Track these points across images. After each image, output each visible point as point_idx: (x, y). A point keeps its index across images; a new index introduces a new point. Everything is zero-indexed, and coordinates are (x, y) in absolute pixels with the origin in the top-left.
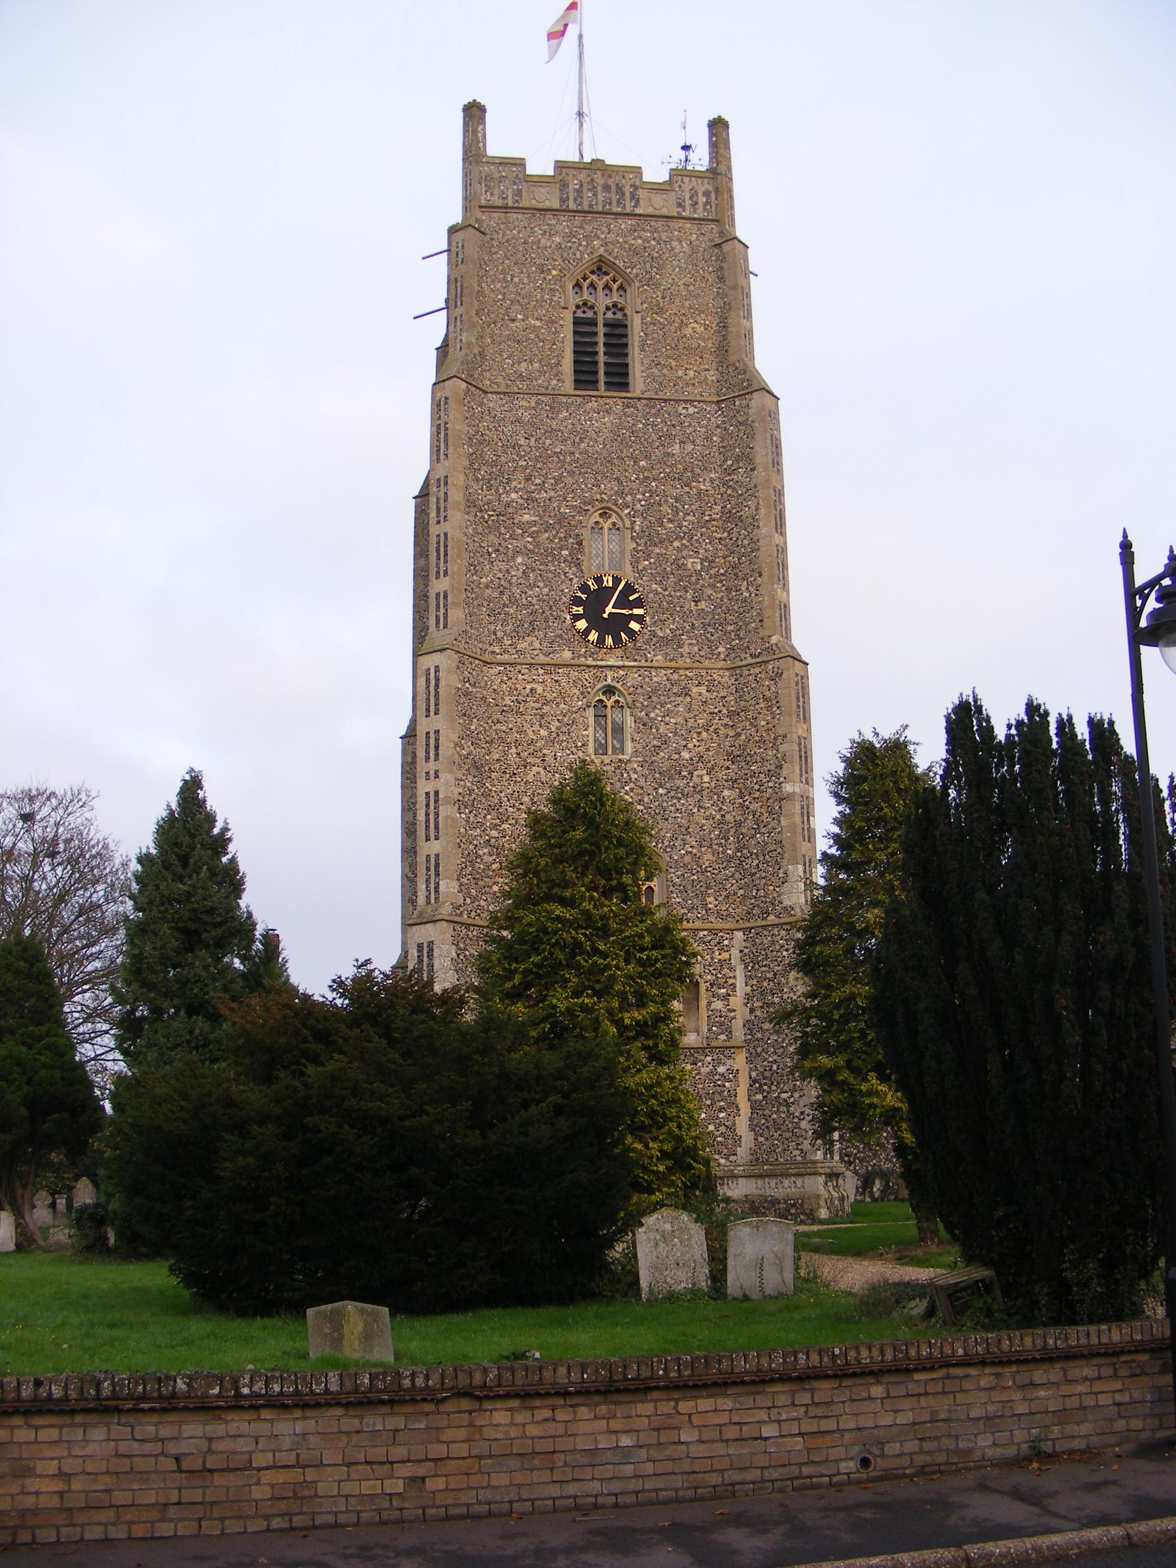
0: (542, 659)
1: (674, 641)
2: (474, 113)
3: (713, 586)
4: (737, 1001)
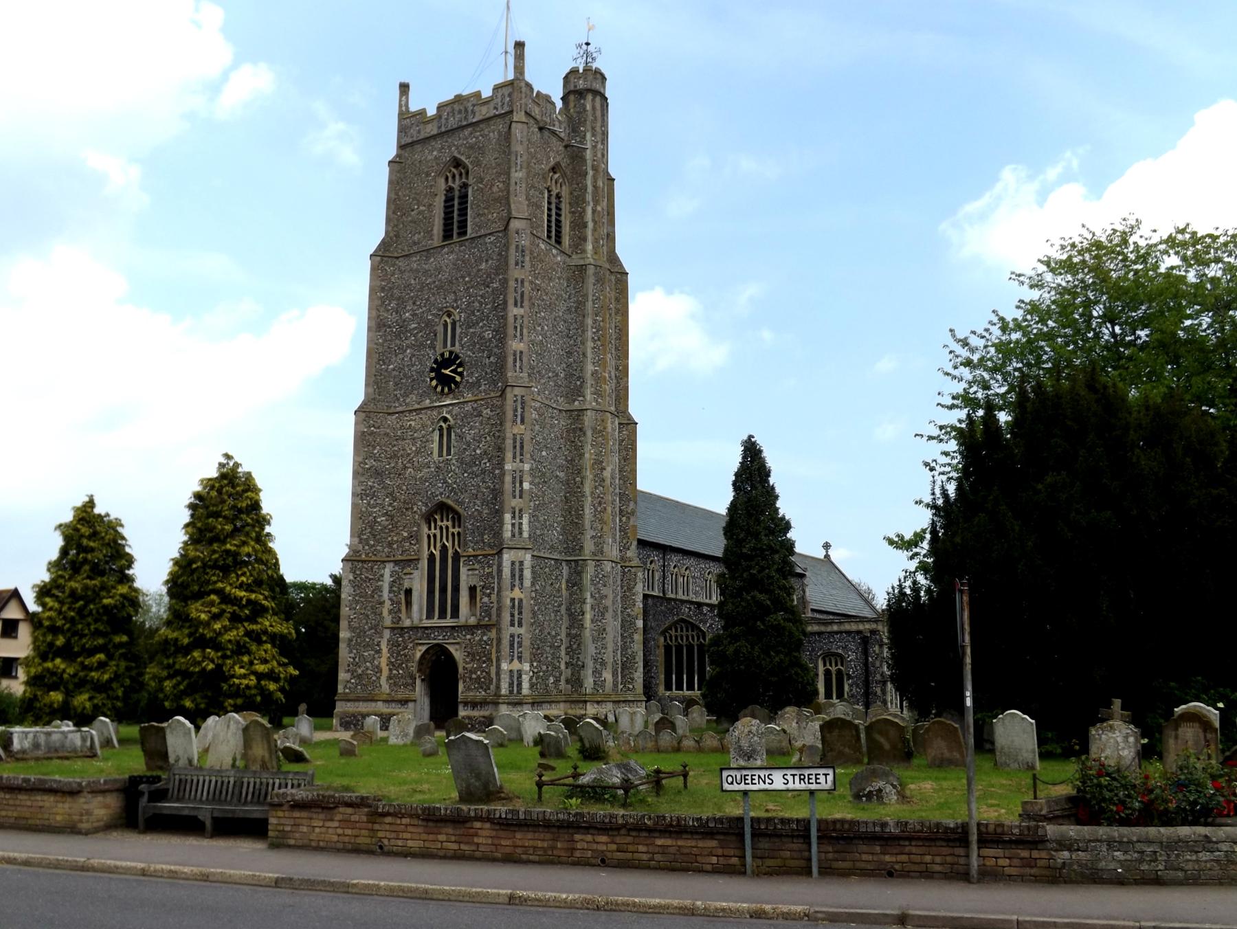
0: (417, 406)
1: (477, 384)
2: (404, 88)
3: (497, 346)
4: (494, 597)
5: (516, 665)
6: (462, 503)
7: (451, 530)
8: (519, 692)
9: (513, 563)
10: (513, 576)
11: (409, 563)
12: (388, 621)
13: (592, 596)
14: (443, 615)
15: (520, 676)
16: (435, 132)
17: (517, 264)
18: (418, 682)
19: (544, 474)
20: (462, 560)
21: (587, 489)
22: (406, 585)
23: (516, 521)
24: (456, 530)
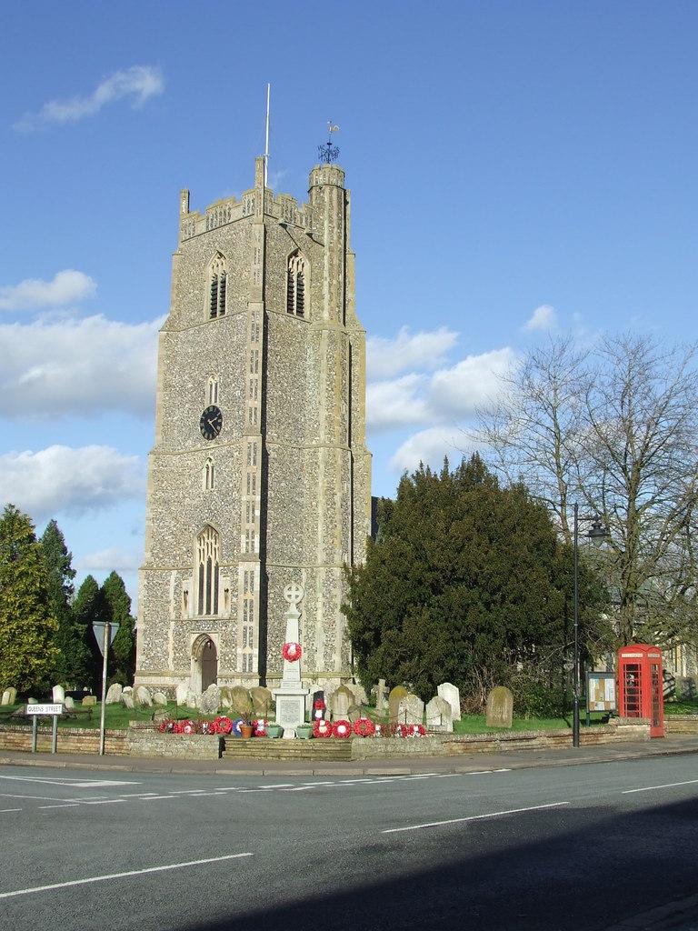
5: (248, 650)
6: (220, 525)
7: (214, 546)
8: (250, 670)
9: (246, 573)
10: (246, 582)
11: (185, 571)
12: (173, 617)
13: (324, 596)
14: (208, 613)
15: (251, 659)
16: (204, 230)
17: (253, 339)
18: (192, 661)
19: (283, 501)
20: (220, 568)
21: (320, 511)
22: (184, 589)
23: (250, 540)
24: (217, 546)
